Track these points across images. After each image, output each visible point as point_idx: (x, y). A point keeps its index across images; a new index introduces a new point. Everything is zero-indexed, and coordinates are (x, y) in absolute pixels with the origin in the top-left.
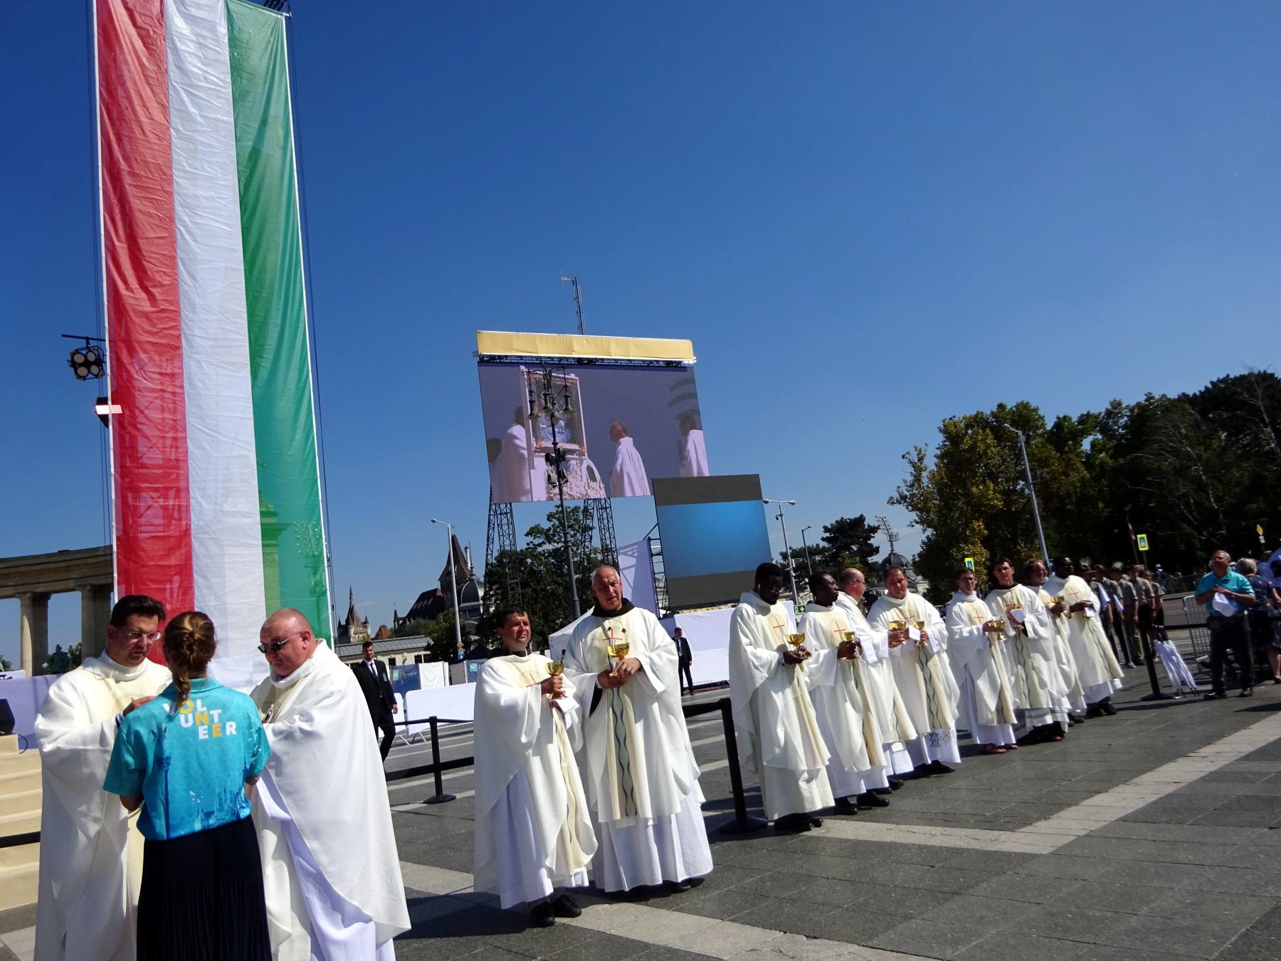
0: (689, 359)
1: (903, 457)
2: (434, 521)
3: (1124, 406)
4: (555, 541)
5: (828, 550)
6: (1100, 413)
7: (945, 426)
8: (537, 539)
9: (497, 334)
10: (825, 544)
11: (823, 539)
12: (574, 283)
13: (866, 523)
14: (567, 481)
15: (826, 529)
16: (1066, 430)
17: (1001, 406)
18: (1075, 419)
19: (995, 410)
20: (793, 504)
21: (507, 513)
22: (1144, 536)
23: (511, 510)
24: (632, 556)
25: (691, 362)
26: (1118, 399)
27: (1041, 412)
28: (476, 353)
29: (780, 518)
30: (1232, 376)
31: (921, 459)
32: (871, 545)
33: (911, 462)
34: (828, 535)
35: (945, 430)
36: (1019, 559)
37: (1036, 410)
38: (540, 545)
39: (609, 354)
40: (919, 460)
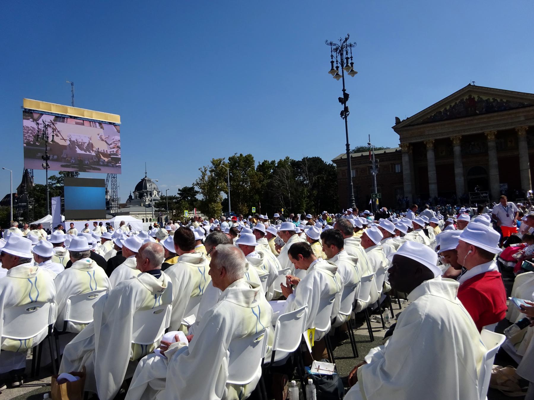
0: (118, 121)
1: (199, 169)
2: (4, 169)
3: (290, 159)
4: (62, 183)
5: (178, 198)
6: (273, 162)
7: (213, 161)
8: (54, 181)
9: (33, 101)
10: (178, 196)
11: (178, 194)
12: (72, 84)
13: (195, 189)
14: (49, 167)
15: (179, 190)
16: (265, 166)
17: (241, 155)
18: (270, 162)
19: (239, 156)
20: (157, 181)
21: (31, 173)
22: (255, 208)
23: (33, 172)
24: (55, 201)
25: (119, 123)
26: (288, 156)
27: (254, 159)
28: (22, 107)
29: (151, 186)
30: (308, 157)
31: (205, 171)
32: (196, 198)
33: (202, 172)
34: (180, 192)
35: (213, 162)
36: (239, 209)
37: (253, 158)
38: (55, 184)
39: (84, 116)
40: (205, 171)
